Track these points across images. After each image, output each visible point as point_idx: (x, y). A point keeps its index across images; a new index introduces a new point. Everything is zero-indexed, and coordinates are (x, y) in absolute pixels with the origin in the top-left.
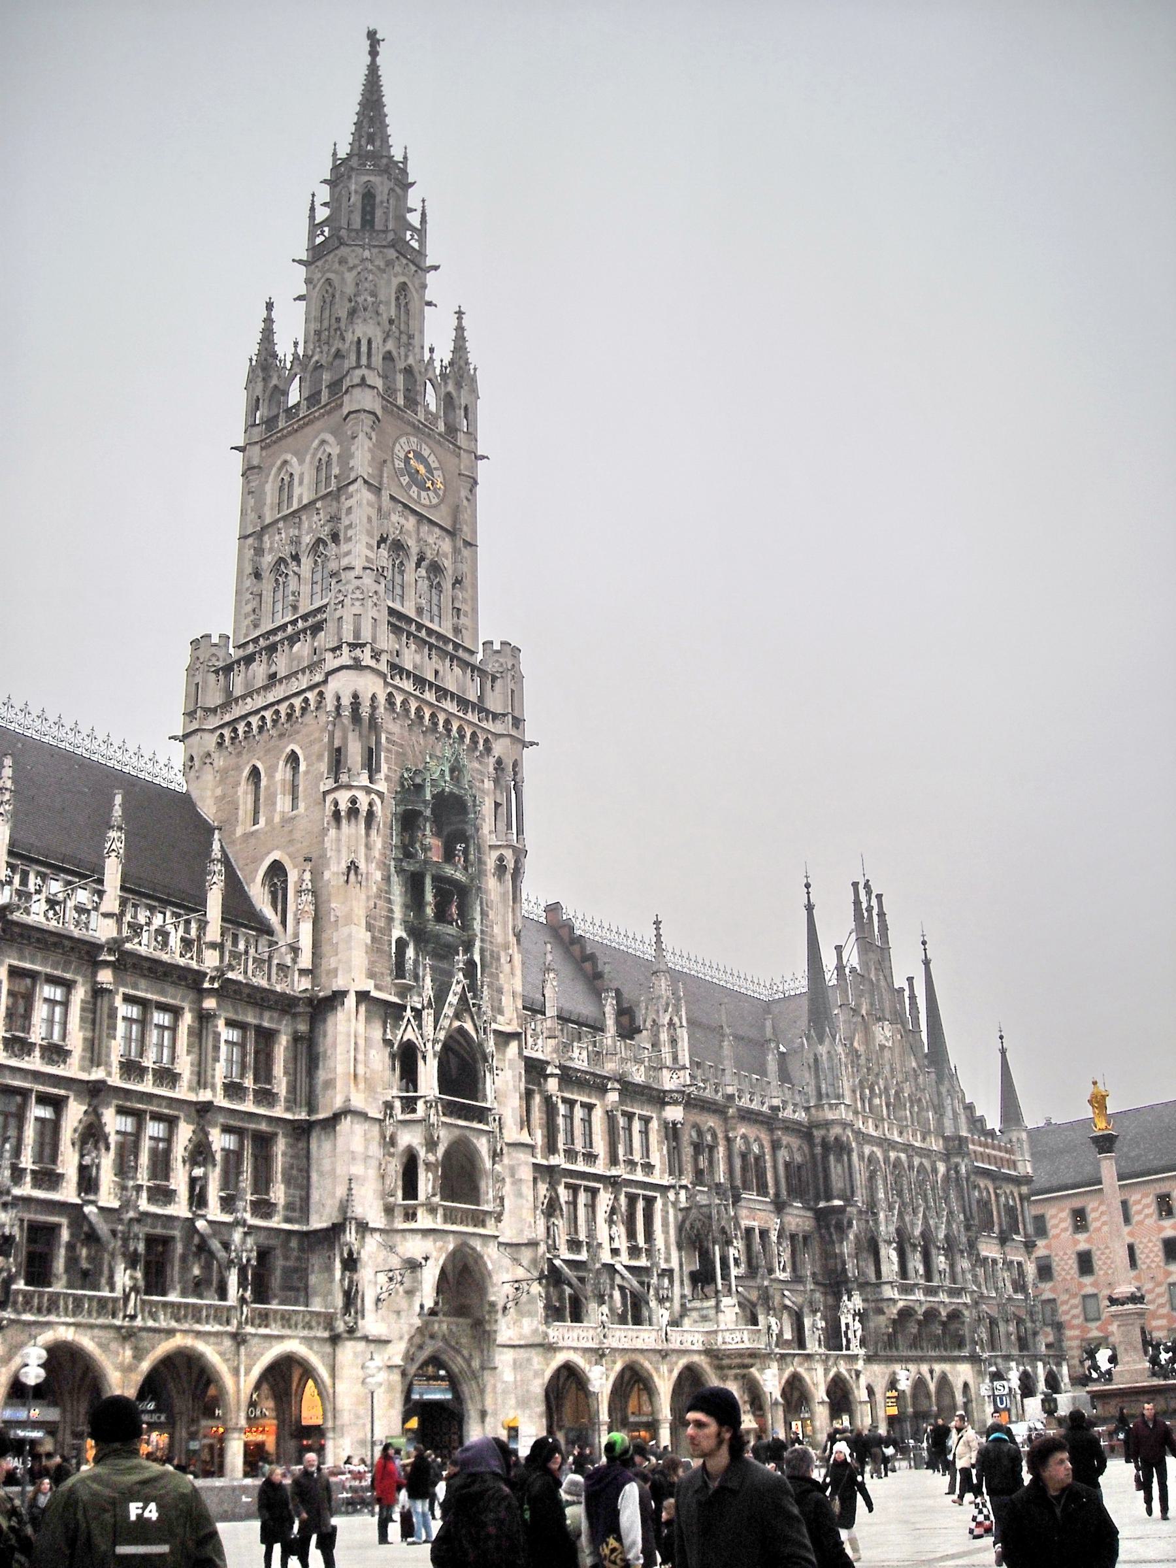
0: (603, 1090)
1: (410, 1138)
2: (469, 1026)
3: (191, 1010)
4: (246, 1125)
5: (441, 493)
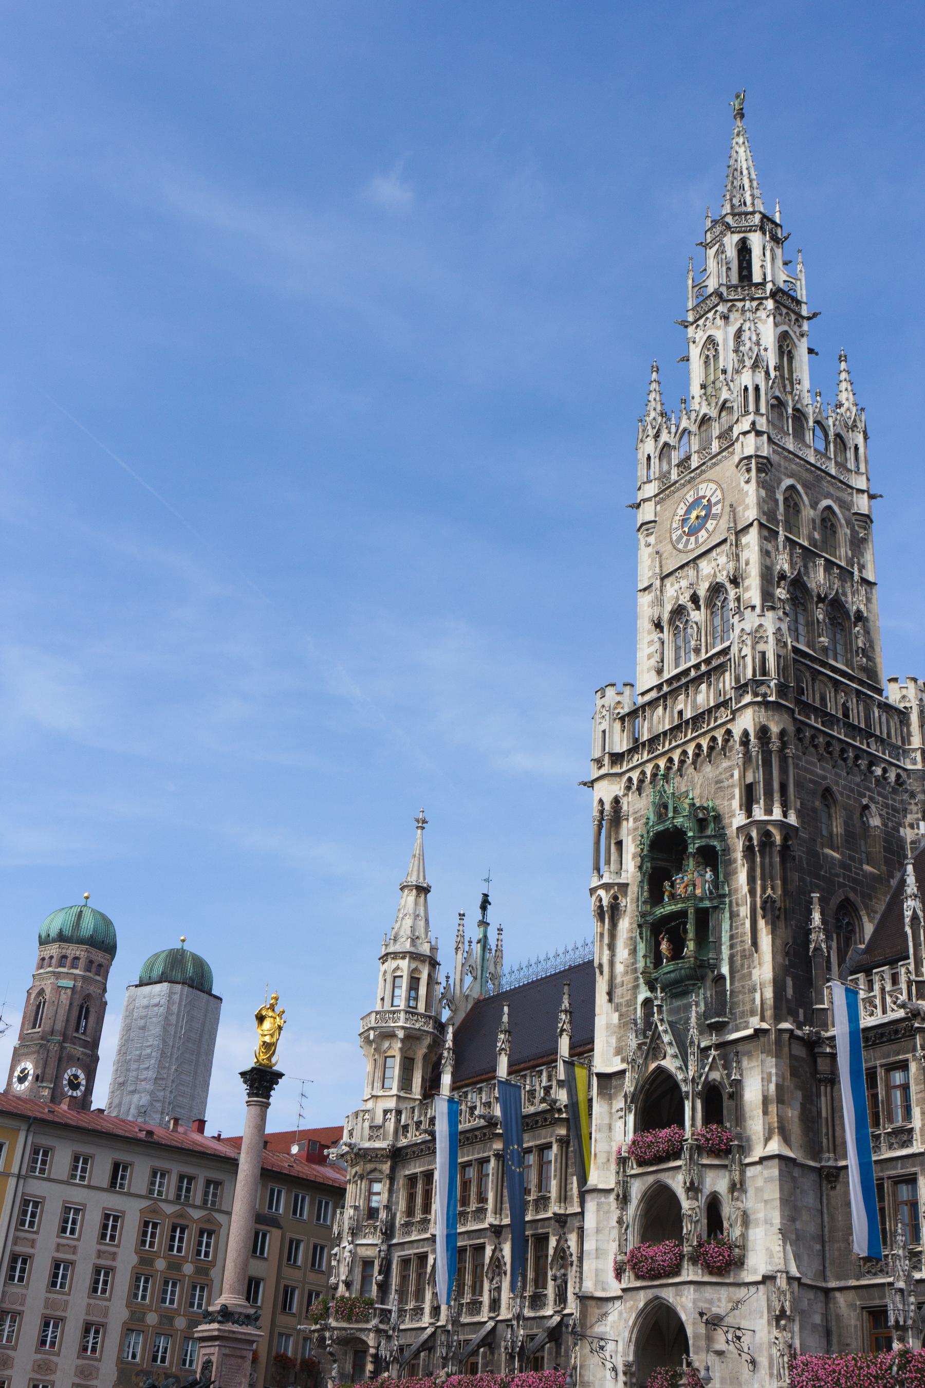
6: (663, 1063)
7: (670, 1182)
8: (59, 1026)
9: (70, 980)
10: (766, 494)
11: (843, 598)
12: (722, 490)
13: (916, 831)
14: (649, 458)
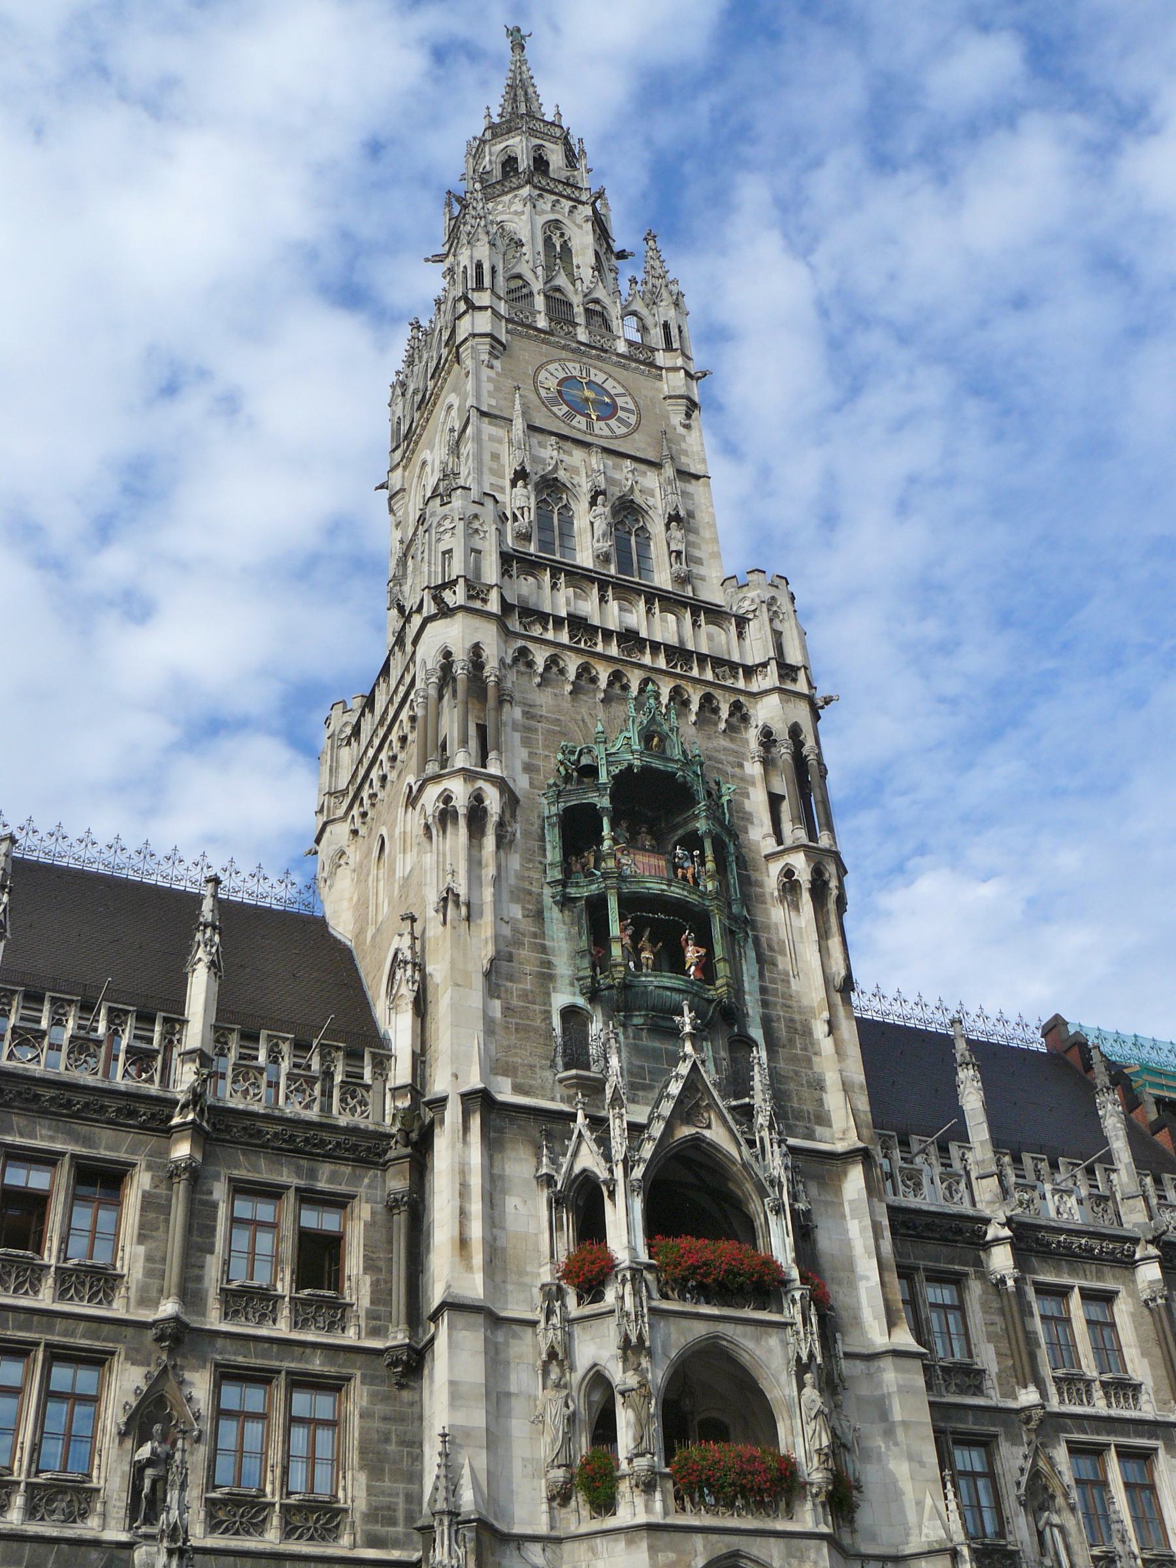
0: (1129, 1264)
1: (597, 1348)
2: (717, 1134)
3: (149, 1168)
4: (275, 1364)
5: (633, 419)
6: (707, 1133)
7: (749, 1344)
12: (635, 402)
14: (493, 270)
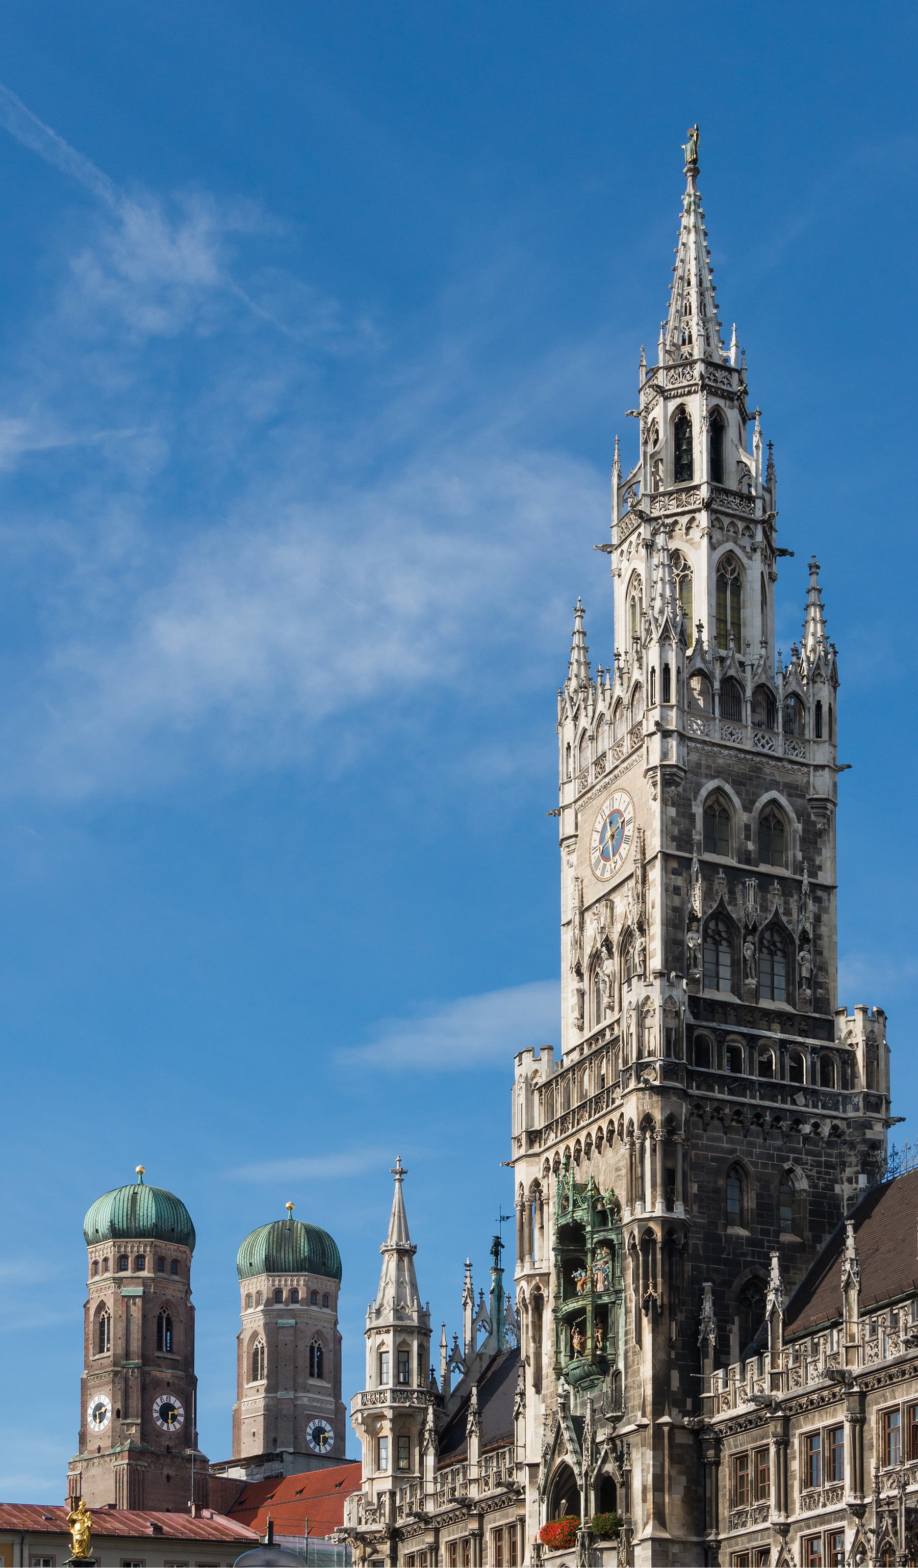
8: (135, 1346)
9: (137, 1286)
10: (677, 811)
11: (784, 919)
13: (854, 1185)
